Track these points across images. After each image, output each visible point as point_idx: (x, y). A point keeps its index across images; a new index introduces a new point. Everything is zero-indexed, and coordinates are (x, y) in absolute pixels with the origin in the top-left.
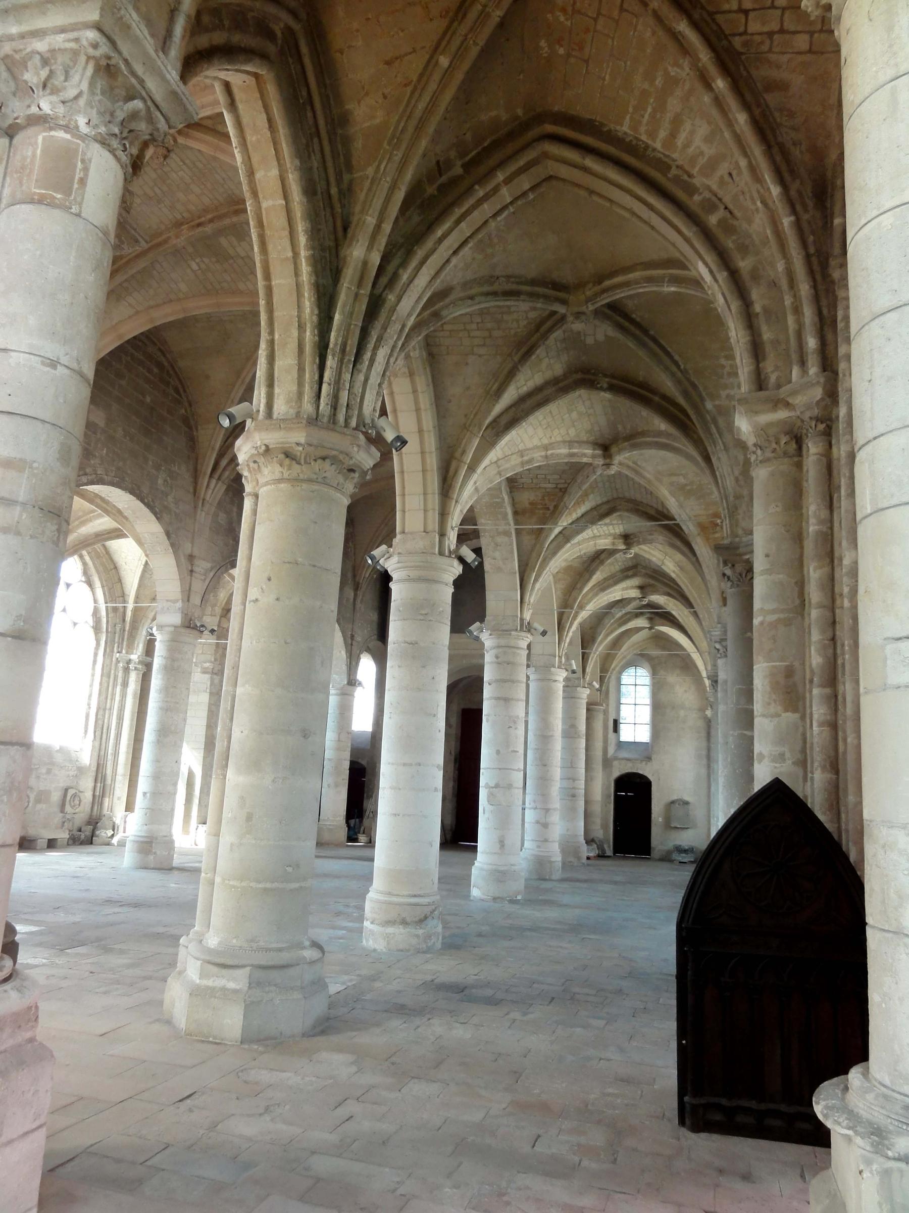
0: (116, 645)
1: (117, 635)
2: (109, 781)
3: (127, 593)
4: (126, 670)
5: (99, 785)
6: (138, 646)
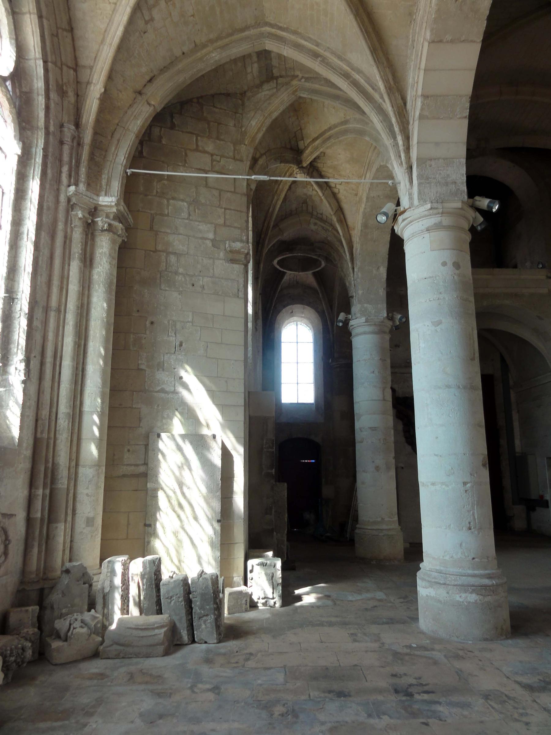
0: (65, 169)
1: (66, 149)
2: (63, 483)
3: (84, 61)
4: (89, 228)
5: (40, 492)
6: (108, 183)
